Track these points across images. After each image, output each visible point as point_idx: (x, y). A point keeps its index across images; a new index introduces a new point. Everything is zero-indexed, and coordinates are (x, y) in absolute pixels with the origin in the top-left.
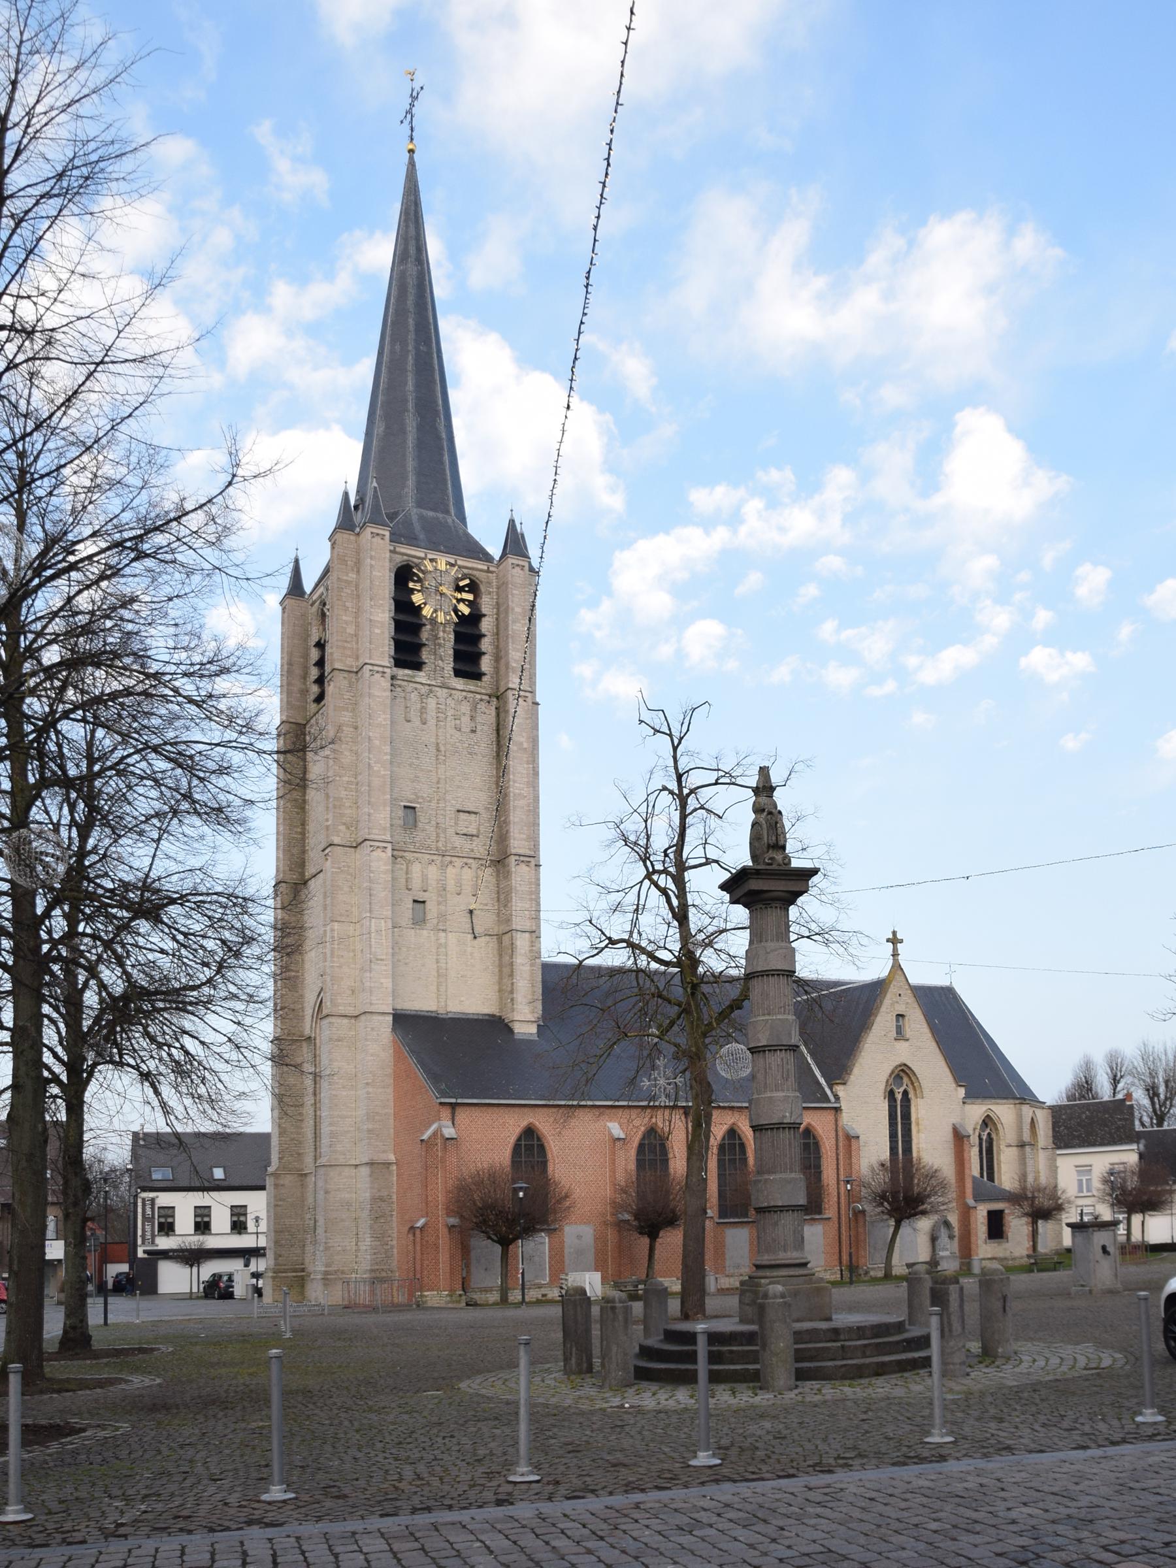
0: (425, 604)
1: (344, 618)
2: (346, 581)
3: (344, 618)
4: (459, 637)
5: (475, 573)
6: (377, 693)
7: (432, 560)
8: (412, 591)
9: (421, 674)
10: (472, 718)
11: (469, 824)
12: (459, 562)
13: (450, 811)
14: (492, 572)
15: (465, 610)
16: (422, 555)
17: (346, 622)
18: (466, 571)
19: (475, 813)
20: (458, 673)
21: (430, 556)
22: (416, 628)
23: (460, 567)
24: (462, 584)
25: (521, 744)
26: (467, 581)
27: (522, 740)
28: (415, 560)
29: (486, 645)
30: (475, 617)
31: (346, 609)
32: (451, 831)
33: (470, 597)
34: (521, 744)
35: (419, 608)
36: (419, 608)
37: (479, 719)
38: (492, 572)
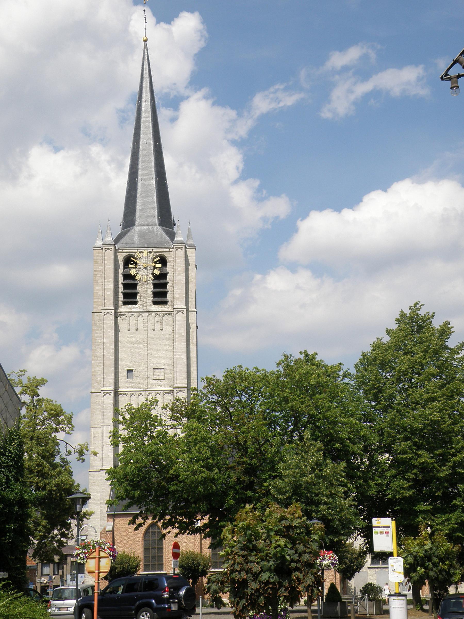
0: (137, 274)
1: (97, 288)
2: (98, 271)
3: (97, 288)
4: (156, 286)
5: (163, 253)
6: (108, 322)
7: (140, 252)
8: (130, 269)
9: (137, 306)
10: (161, 323)
11: (160, 374)
12: (154, 250)
13: (150, 368)
14: (171, 251)
15: (157, 272)
16: (136, 251)
17: (99, 290)
18: (157, 254)
19: (163, 368)
20: (155, 303)
21: (139, 251)
22: (135, 286)
23: (155, 252)
24: (155, 260)
25: (181, 333)
26: (158, 258)
27: (181, 331)
28: (133, 254)
29: (169, 286)
30: (164, 276)
31: (98, 284)
32: (151, 378)
33: (160, 265)
34: (181, 333)
35: (134, 276)
36: (134, 276)
37: (164, 323)
38: (171, 251)
